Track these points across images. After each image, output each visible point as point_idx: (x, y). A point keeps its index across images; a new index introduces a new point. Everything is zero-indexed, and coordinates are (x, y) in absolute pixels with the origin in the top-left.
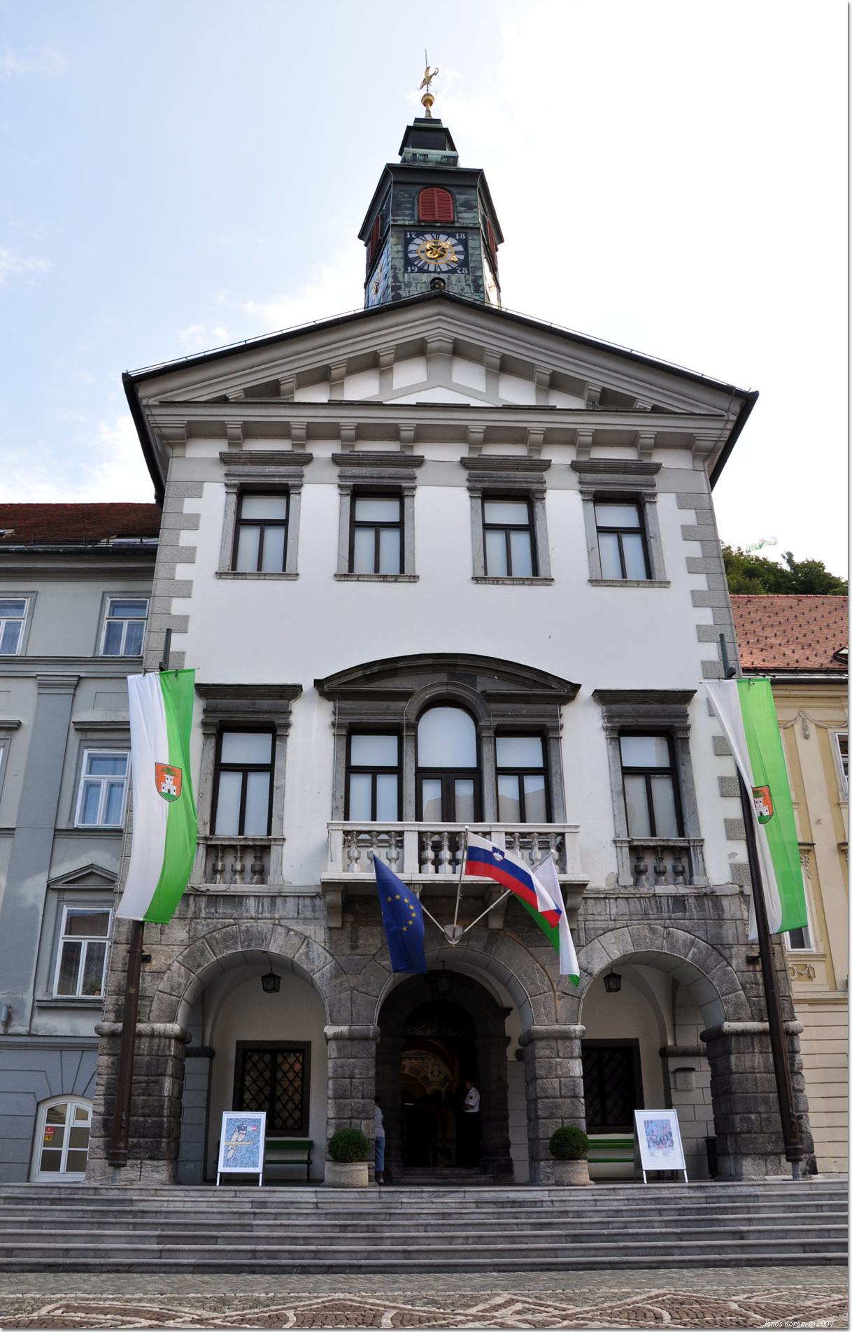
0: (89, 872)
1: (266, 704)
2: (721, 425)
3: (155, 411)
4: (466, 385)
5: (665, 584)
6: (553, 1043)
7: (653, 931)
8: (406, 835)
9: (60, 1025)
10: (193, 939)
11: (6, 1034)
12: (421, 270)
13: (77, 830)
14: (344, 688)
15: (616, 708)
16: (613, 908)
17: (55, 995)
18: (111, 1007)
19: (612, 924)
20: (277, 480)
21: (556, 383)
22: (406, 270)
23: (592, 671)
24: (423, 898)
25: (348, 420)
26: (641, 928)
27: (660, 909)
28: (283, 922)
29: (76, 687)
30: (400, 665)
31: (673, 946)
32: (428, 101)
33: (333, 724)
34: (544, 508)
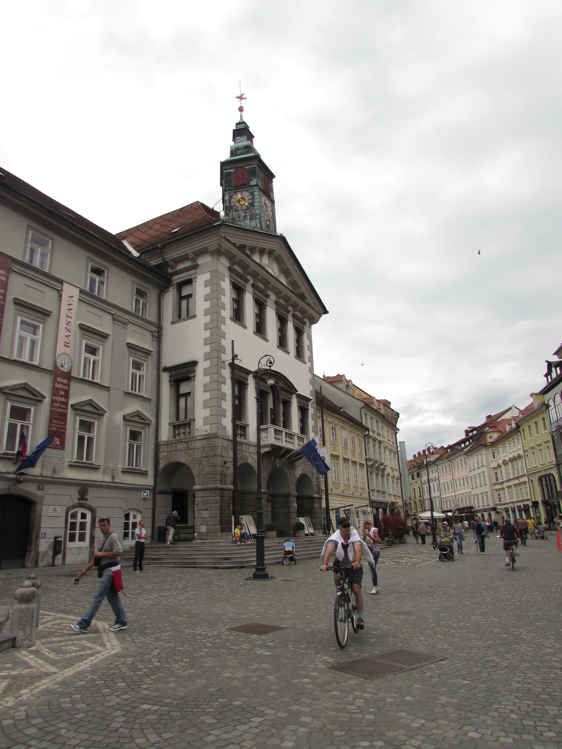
0: (138, 414)
1: (244, 375)
3: (222, 240)
4: (274, 270)
5: (305, 363)
9: (129, 479)
11: (113, 482)
13: (130, 393)
15: (301, 400)
17: (127, 466)
18: (219, 479)
20: (240, 285)
21: (293, 284)
25: (262, 274)
28: (251, 454)
29: (126, 324)
32: (241, 109)
33: (256, 388)
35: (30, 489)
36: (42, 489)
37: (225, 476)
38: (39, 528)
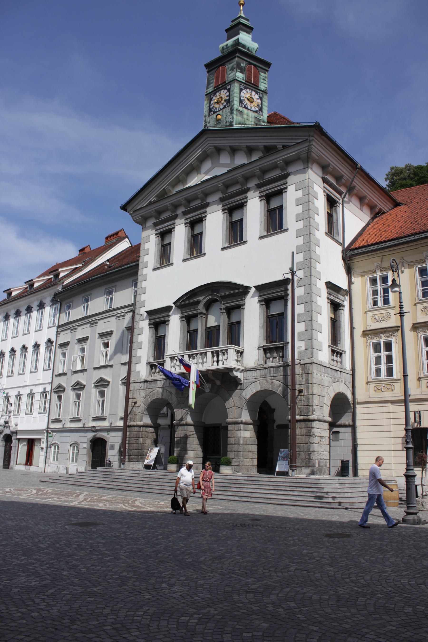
2: (307, 144)
6: (233, 425)
7: (267, 382)
8: (185, 356)
10: (146, 396)
12: (214, 112)
14: (181, 304)
16: (255, 374)
19: (254, 380)
22: (209, 116)
23: (251, 279)
24: (212, 373)
25: (182, 197)
26: (263, 381)
27: (270, 373)
28: (166, 388)
30: (196, 291)
31: (273, 387)
34: (246, 209)
35: (103, 435)
36: (108, 434)
37: (135, 414)
38: (108, 455)
